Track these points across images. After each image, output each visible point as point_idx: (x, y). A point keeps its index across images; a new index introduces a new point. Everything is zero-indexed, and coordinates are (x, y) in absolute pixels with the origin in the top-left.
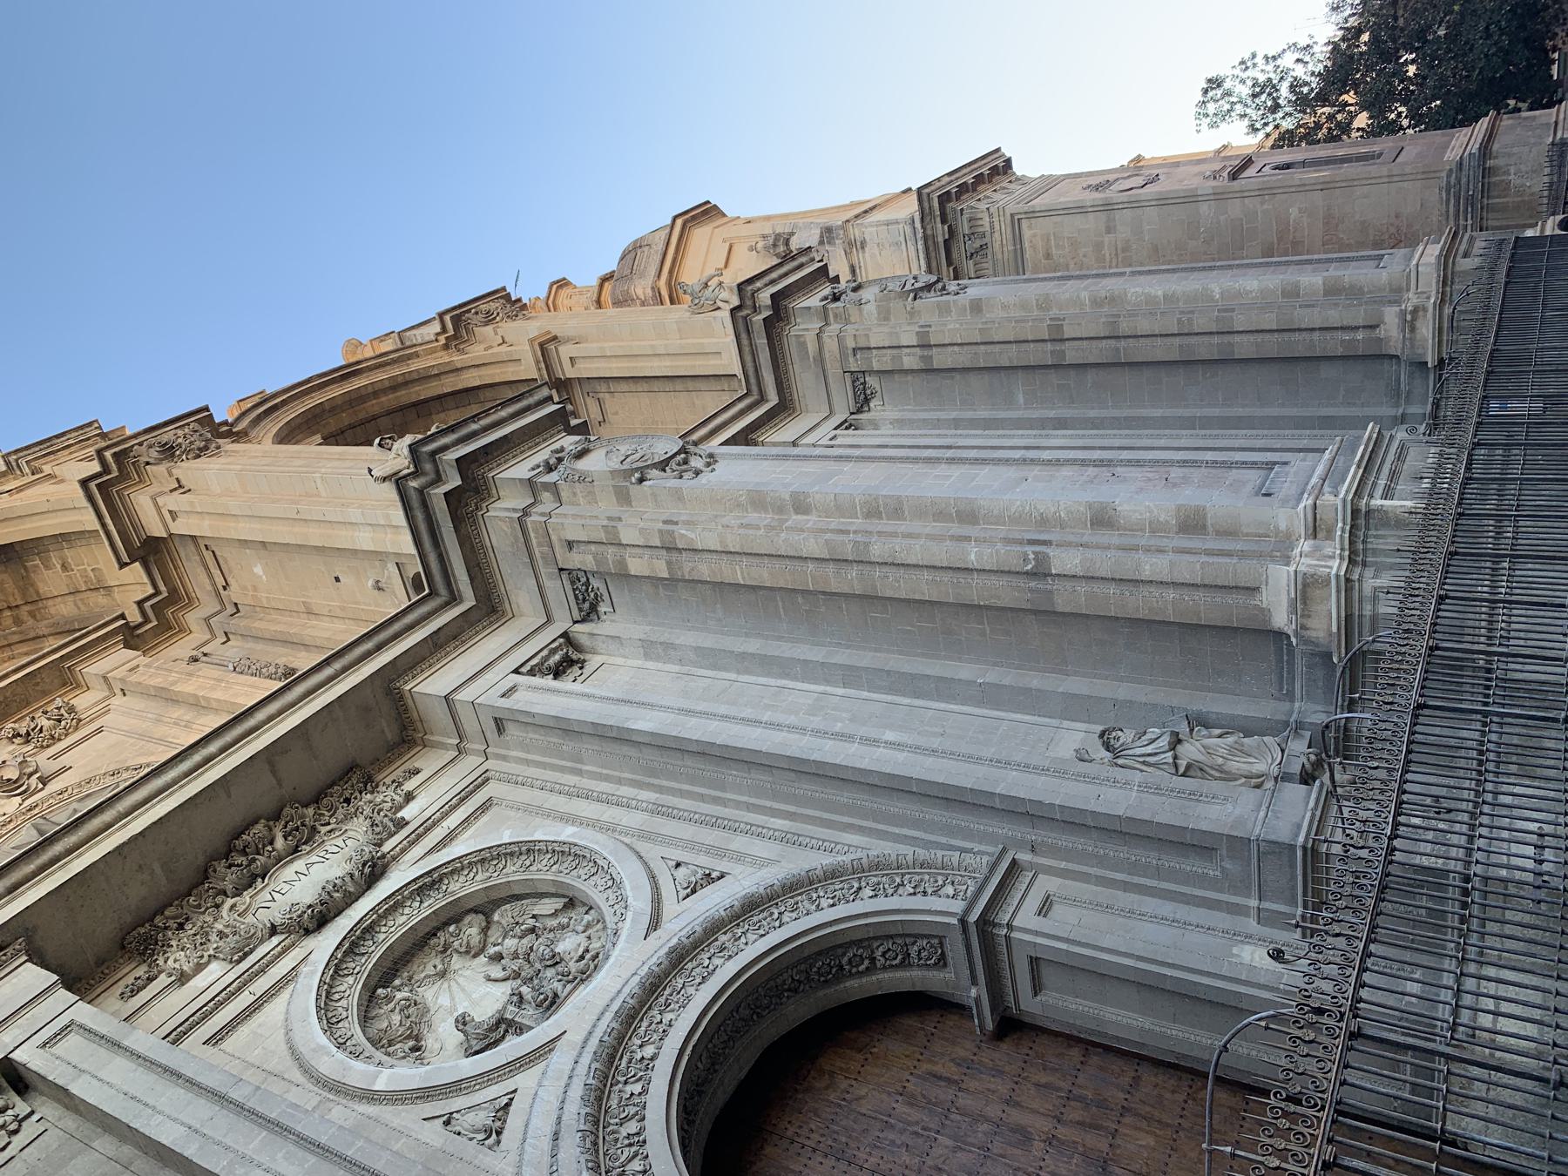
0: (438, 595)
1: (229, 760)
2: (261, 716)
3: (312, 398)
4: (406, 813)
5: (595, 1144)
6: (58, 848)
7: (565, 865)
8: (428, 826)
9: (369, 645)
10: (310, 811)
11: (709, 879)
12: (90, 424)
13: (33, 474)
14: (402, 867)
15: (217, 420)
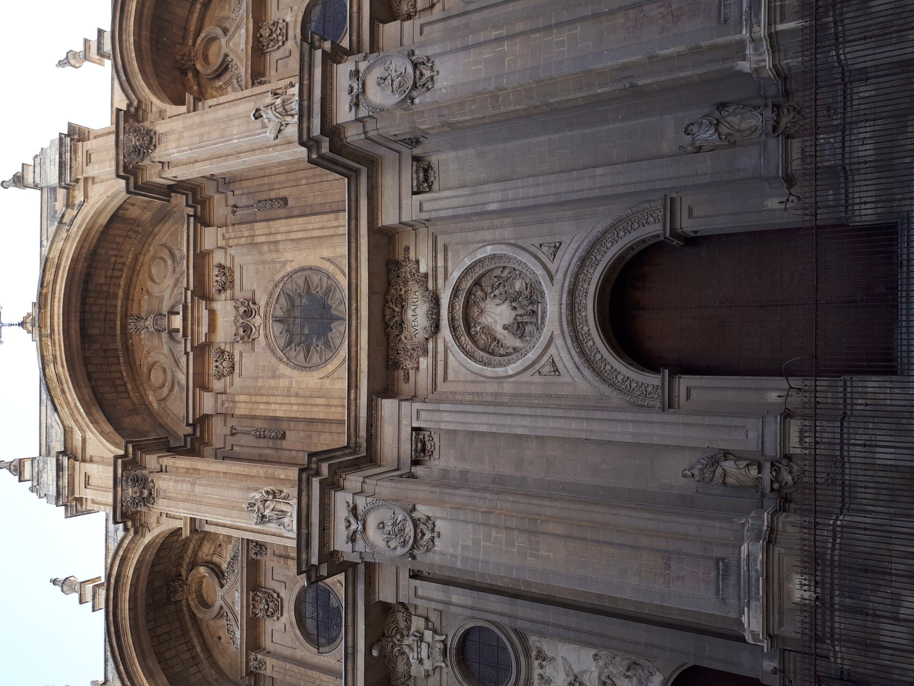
0: (351, 176)
1: (362, 303)
2: (354, 281)
3: (126, 40)
4: (423, 269)
5: (592, 367)
6: (353, 368)
7: (496, 260)
8: (435, 269)
9: (353, 222)
10: (393, 291)
11: (557, 248)
12: (61, 139)
13: (77, 183)
14: (442, 291)
15: (125, 109)
